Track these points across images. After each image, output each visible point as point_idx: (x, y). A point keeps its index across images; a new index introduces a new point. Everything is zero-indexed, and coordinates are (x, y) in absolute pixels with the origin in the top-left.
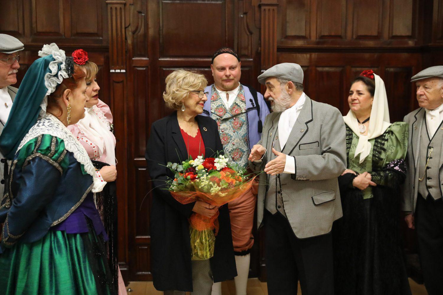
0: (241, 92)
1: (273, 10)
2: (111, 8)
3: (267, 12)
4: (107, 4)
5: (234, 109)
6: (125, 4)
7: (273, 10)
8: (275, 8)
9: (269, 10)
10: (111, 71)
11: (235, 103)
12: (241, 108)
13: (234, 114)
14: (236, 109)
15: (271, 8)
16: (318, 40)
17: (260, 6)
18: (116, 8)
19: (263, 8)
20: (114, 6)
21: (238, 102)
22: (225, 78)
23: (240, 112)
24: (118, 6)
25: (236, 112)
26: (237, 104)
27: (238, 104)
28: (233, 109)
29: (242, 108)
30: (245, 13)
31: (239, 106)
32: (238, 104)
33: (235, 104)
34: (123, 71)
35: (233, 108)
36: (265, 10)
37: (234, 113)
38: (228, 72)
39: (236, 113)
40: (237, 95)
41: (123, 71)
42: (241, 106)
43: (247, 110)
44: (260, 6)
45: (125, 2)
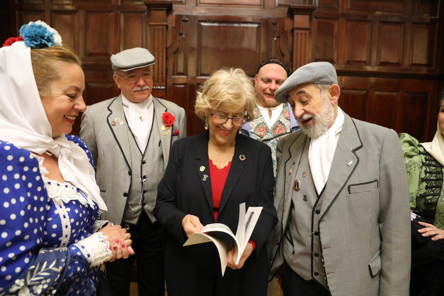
0: (285, 109)
1: (305, 34)
3: (299, 35)
5: (277, 128)
7: (305, 34)
8: (307, 32)
9: (301, 34)
11: (279, 121)
12: (286, 127)
13: (277, 135)
14: (279, 128)
15: (304, 32)
17: (292, 31)
19: (295, 32)
21: (283, 120)
22: (268, 91)
23: (284, 132)
25: (279, 132)
26: (281, 122)
27: (282, 122)
28: (276, 128)
29: (287, 127)
31: (283, 124)
32: (282, 122)
33: (279, 122)
35: (275, 127)
36: (297, 34)
37: (277, 133)
38: (273, 86)
39: (279, 133)
40: (281, 111)
42: (286, 125)
43: (292, 129)
44: (292, 31)
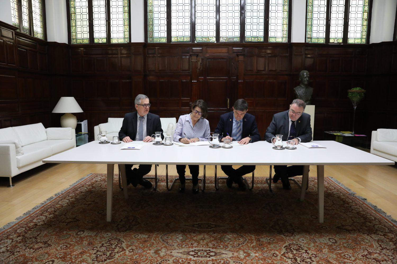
1: (242, 62)
2: (193, 63)
4: (192, 61)
6: (197, 61)
7: (242, 62)
9: (241, 62)
10: (193, 81)
16: (256, 71)
17: (238, 61)
18: (194, 63)
19: (239, 62)
20: (193, 62)
24: (195, 62)
30: (234, 63)
34: (196, 81)
36: (240, 62)
41: (196, 81)
45: (196, 60)
